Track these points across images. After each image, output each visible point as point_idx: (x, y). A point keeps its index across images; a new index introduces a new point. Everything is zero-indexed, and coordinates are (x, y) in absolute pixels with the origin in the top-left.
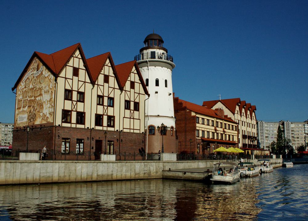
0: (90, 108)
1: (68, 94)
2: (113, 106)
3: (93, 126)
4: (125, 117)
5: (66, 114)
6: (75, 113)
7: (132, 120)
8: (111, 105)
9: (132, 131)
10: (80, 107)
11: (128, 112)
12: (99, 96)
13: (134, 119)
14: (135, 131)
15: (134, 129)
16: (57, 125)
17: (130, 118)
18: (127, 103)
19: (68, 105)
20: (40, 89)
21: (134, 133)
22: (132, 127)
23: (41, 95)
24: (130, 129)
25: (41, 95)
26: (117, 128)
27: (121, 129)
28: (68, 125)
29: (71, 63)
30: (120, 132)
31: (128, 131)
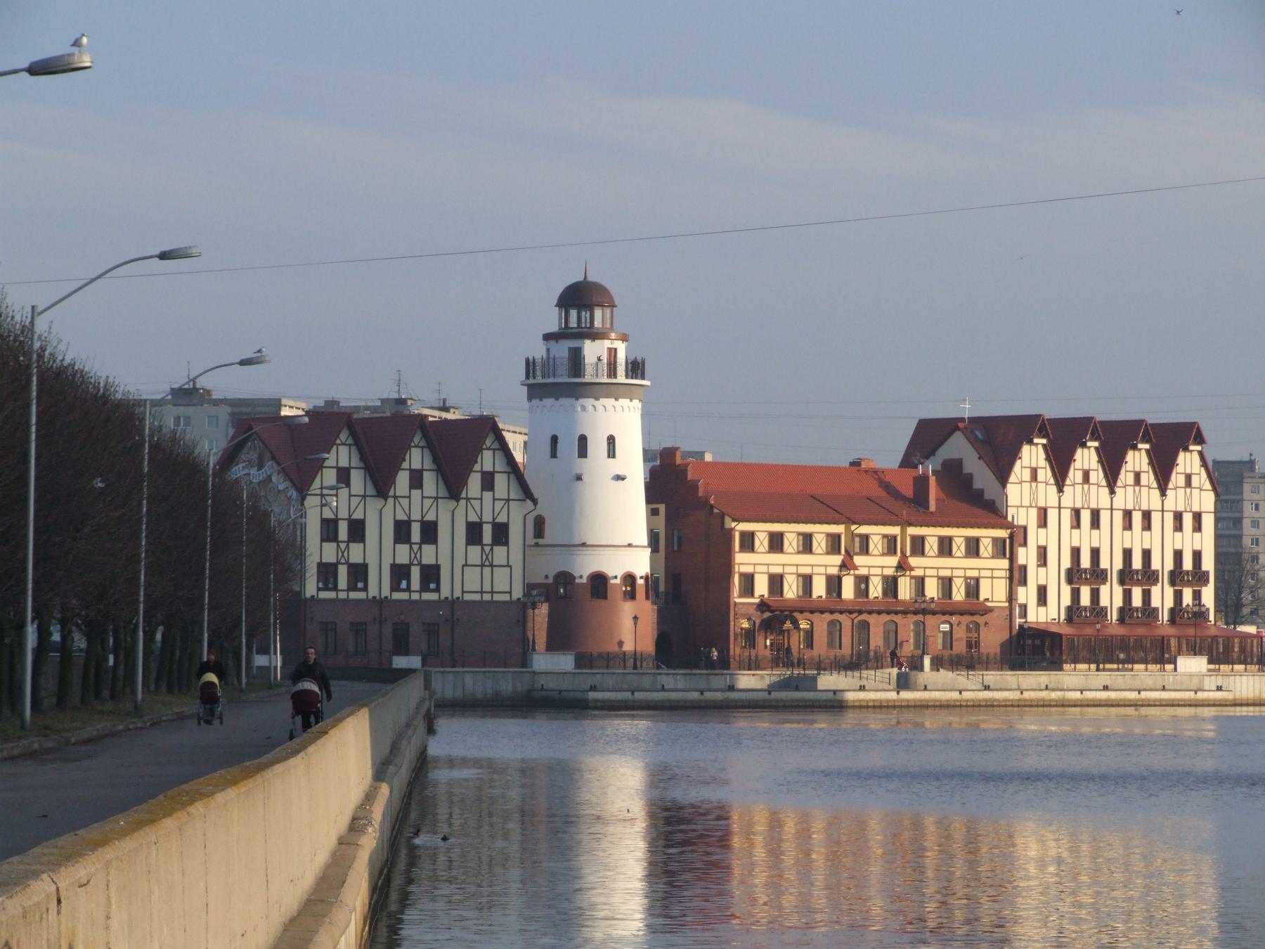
0: (379, 552)
3: (386, 592)
4: (466, 565)
7: (487, 570)
9: (487, 597)
10: (356, 554)
11: (475, 551)
14: (497, 597)
16: (308, 595)
17: (482, 565)
18: (474, 533)
19: (330, 553)
21: (492, 602)
22: (487, 587)
24: (482, 592)
26: (445, 592)
27: (457, 593)
28: (330, 595)
30: (452, 603)
31: (477, 597)
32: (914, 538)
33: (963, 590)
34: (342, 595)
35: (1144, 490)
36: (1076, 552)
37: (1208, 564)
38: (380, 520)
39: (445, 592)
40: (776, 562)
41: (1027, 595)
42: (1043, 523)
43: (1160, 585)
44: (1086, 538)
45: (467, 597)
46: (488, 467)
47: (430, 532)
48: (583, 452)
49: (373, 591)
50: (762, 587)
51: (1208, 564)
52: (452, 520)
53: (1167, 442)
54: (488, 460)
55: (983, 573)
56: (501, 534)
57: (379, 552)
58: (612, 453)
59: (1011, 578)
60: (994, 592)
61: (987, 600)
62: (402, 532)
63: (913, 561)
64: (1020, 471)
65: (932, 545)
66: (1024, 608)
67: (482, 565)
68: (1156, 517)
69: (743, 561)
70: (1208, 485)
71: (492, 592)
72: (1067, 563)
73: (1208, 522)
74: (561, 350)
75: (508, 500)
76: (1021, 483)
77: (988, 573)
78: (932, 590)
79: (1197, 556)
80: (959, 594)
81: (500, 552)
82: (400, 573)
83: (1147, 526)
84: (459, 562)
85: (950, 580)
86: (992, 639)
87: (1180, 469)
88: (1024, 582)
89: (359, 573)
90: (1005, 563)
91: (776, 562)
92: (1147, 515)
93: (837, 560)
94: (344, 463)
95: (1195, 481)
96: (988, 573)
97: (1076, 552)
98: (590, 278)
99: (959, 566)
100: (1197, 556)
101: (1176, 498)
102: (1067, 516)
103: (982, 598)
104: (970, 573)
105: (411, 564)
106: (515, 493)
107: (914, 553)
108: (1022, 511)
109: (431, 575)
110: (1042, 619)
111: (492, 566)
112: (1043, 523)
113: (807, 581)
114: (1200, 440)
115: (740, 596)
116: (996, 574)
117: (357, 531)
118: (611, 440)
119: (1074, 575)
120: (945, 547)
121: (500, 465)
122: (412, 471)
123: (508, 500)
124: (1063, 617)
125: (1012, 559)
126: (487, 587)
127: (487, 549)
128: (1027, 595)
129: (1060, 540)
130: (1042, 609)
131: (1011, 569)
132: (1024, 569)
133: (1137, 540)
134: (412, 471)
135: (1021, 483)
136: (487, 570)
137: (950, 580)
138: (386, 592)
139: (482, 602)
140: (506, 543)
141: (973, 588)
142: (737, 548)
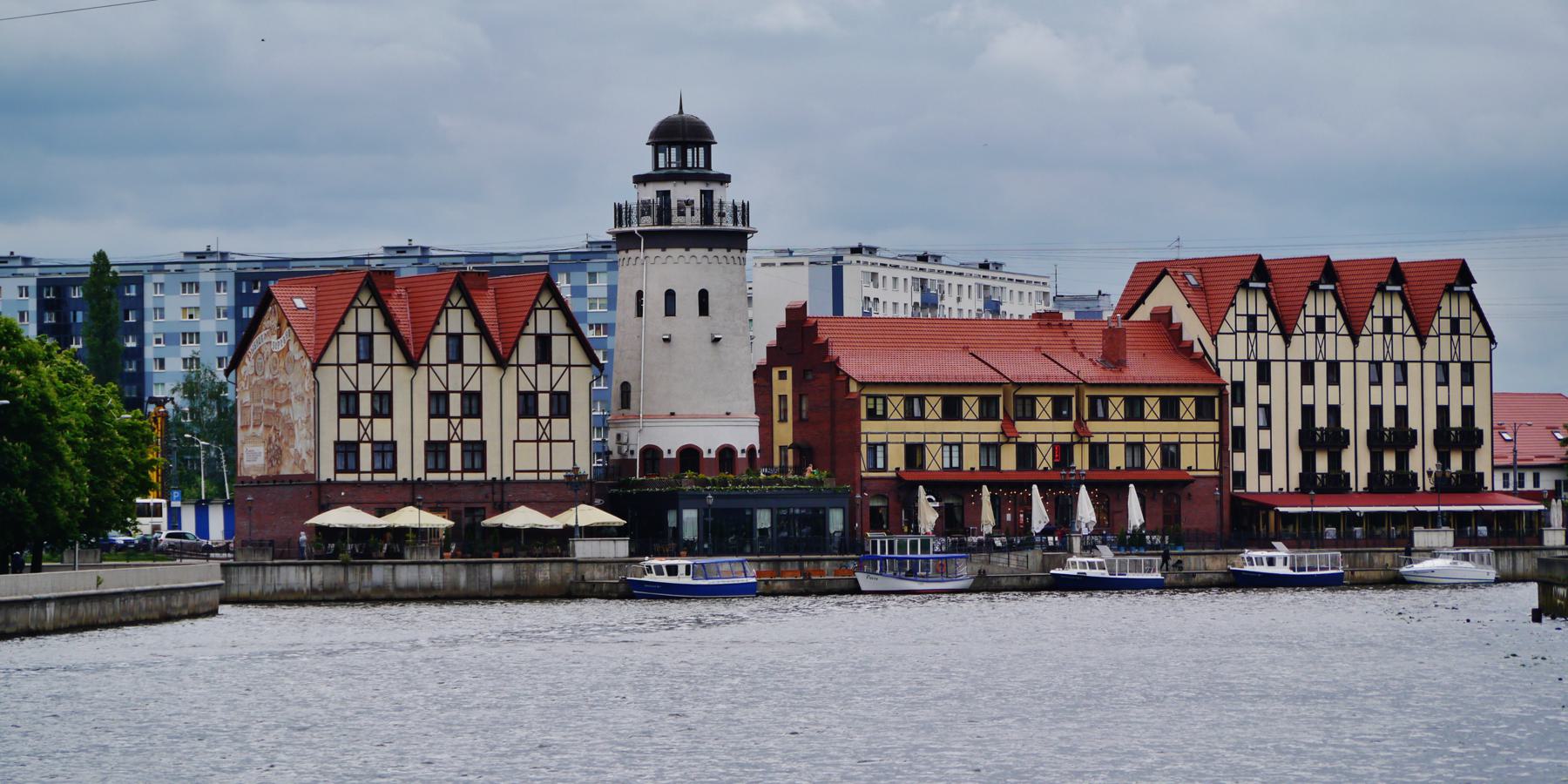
1: (348, 404)
2: (479, 415)
5: (346, 452)
6: (369, 446)
8: (474, 411)
9: (545, 476)
11: (529, 425)
12: (433, 395)
13: (550, 441)
15: (551, 471)
17: (538, 441)
18: (527, 405)
20: (287, 387)
21: (550, 482)
22: (545, 465)
23: (288, 402)
24: (538, 471)
25: (288, 402)
27: (508, 473)
29: (349, 325)
31: (533, 476)
32: (1093, 399)
33: (1158, 458)
34: (366, 478)
36: (1308, 412)
37: (1482, 422)
38: (411, 393)
39: (493, 472)
40: (914, 430)
41: (1247, 461)
42: (1264, 376)
43: (1419, 447)
44: (1321, 395)
45: (519, 477)
46: (543, 329)
47: (473, 404)
48: (670, 310)
49: (403, 472)
50: (897, 459)
52: (500, 391)
54: (544, 322)
55: (1184, 438)
56: (561, 405)
57: (410, 428)
58: (704, 310)
59: (1222, 444)
60: (1199, 458)
61: (1190, 469)
62: (438, 403)
63: (1093, 426)
64: (1235, 320)
66: (1240, 478)
67: (538, 441)
68: (1413, 370)
69: (871, 430)
71: (551, 471)
72: (1296, 423)
75: (569, 366)
76: (1235, 333)
77: (1192, 438)
80: (1153, 461)
81: (560, 425)
82: (436, 452)
83: (1402, 380)
84: (510, 434)
85: (1142, 445)
86: (1201, 514)
88: (1240, 445)
89: (386, 452)
90: (1213, 426)
91: (914, 430)
92: (1402, 366)
93: (995, 426)
94: (365, 327)
96: (1192, 438)
97: (1308, 412)
99: (1153, 429)
100: (1468, 412)
102: (1295, 370)
103: (1183, 466)
104: (1166, 439)
105: (450, 441)
106: (578, 356)
107: (1093, 416)
108: (1238, 366)
109: (476, 452)
110: (1265, 488)
111: (550, 441)
112: (1264, 376)
114: (1464, 275)
115: (870, 470)
116: (1201, 438)
117: (383, 404)
118: (703, 295)
119: (1310, 440)
121: (559, 325)
122: (449, 336)
123: (569, 366)
124: (1295, 483)
125: (1223, 420)
126: (545, 465)
127: (544, 422)
128: (1247, 461)
129: (1287, 397)
130: (1265, 479)
131: (1222, 432)
132: (1240, 433)
133: (1389, 397)
134: (449, 336)
135: (1235, 333)
136: (544, 447)
137: (1142, 445)
138: (419, 473)
139: (538, 482)
140: (567, 415)
141: (1170, 455)
142: (864, 415)
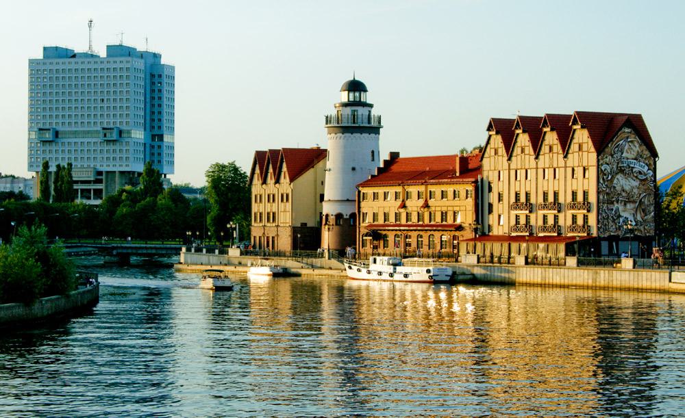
35: (555, 155)
51: (593, 198)
53: (562, 126)
65: (438, 194)
70: (593, 149)
72: (513, 200)
73: (592, 173)
74: (348, 110)
78: (438, 219)
79: (585, 194)
87: (575, 141)
95: (585, 147)
98: (356, 79)
100: (585, 194)
101: (573, 159)
113: (386, 216)
120: (444, 195)
